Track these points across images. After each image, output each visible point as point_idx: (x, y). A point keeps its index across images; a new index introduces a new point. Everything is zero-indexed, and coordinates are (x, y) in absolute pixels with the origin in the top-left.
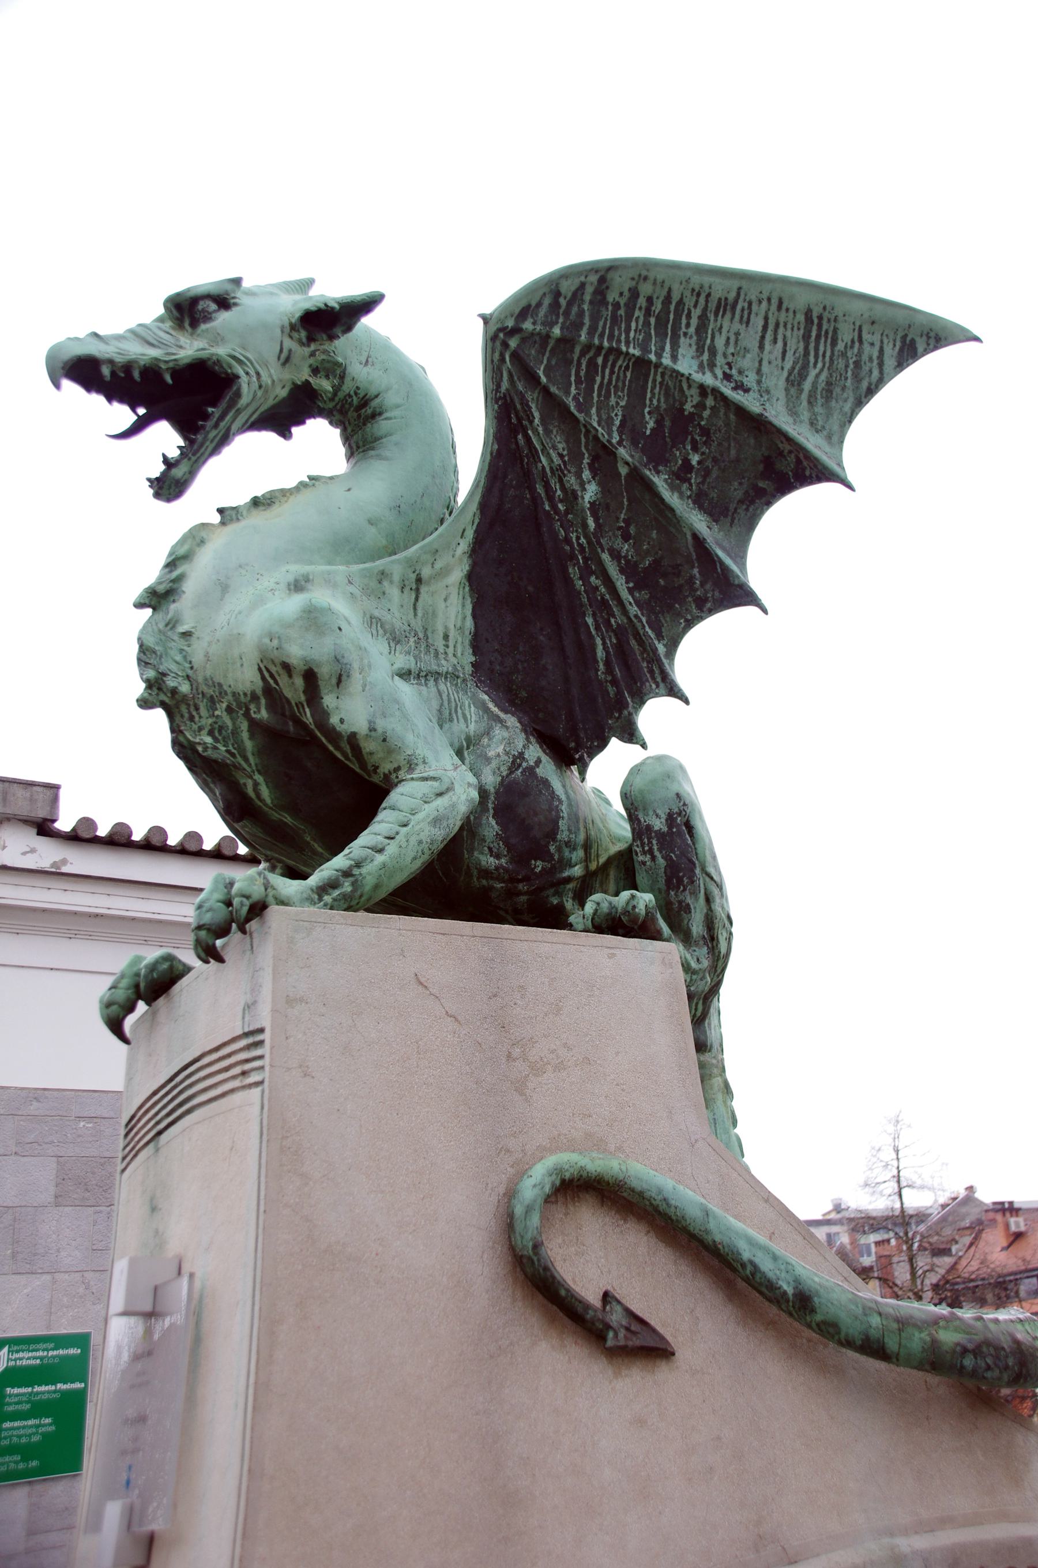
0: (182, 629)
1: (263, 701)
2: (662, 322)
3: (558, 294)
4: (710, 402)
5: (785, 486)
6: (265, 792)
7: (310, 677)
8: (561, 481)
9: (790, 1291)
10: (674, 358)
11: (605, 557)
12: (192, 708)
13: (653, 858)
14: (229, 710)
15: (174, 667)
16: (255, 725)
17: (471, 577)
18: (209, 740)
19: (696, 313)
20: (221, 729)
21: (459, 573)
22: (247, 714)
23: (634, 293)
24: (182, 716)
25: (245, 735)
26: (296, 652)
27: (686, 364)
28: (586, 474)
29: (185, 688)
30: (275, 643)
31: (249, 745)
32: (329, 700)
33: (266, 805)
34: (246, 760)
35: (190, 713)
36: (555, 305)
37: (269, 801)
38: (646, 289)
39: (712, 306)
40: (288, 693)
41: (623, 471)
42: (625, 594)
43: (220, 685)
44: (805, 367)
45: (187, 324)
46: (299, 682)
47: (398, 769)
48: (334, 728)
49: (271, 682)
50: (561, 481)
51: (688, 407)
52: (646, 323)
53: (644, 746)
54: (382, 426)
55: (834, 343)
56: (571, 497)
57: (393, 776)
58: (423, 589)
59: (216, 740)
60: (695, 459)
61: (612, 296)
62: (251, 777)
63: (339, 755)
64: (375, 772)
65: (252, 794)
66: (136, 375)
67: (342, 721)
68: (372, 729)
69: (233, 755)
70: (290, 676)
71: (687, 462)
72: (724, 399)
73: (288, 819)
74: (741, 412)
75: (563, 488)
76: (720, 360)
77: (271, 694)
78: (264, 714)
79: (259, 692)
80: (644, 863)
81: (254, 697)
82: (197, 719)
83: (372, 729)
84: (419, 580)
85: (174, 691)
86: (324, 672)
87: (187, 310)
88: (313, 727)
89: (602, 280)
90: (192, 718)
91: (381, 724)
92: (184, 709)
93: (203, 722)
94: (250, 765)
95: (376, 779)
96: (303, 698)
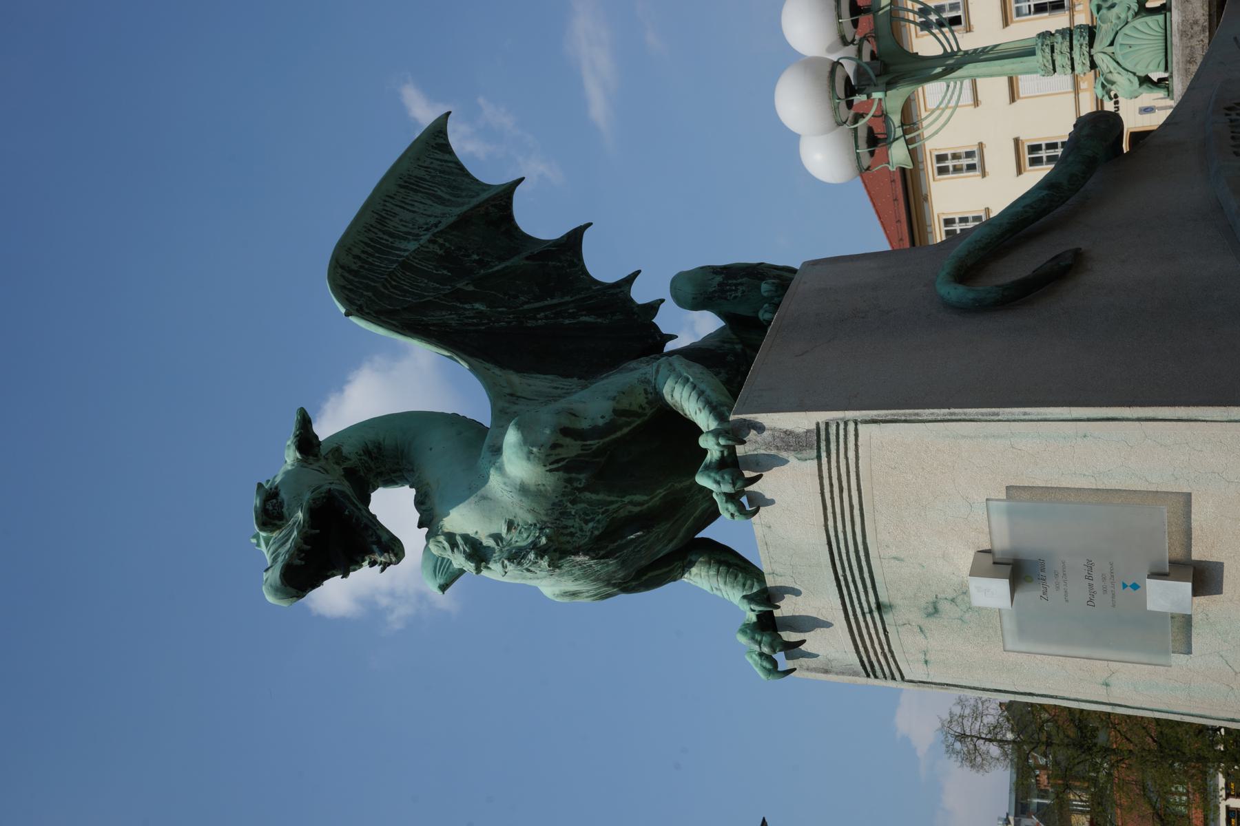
0: (504, 531)
1: (573, 475)
3: (344, 287)
4: (441, 241)
5: (510, 218)
6: (638, 498)
7: (566, 432)
9: (1045, 192)
10: (405, 251)
11: (526, 307)
12: (565, 532)
13: (741, 284)
14: (573, 502)
17: (519, 370)
18: (591, 525)
21: (515, 378)
22: (580, 490)
23: (356, 257)
25: (594, 497)
27: (412, 246)
31: (601, 497)
32: (585, 425)
33: (647, 502)
35: (567, 535)
36: (350, 290)
37: (646, 498)
38: (356, 251)
42: (555, 301)
43: (554, 504)
44: (433, 195)
52: (379, 258)
53: (662, 301)
55: (425, 180)
59: (592, 520)
60: (475, 257)
61: (354, 267)
63: (626, 430)
64: (644, 409)
67: (603, 417)
68: (614, 399)
71: (475, 261)
72: (441, 232)
73: (661, 492)
74: (453, 226)
76: (415, 231)
79: (566, 476)
81: (569, 481)
83: (614, 399)
84: (512, 395)
86: (566, 422)
88: (601, 442)
89: (342, 267)
90: (572, 534)
93: (577, 525)
95: (649, 412)
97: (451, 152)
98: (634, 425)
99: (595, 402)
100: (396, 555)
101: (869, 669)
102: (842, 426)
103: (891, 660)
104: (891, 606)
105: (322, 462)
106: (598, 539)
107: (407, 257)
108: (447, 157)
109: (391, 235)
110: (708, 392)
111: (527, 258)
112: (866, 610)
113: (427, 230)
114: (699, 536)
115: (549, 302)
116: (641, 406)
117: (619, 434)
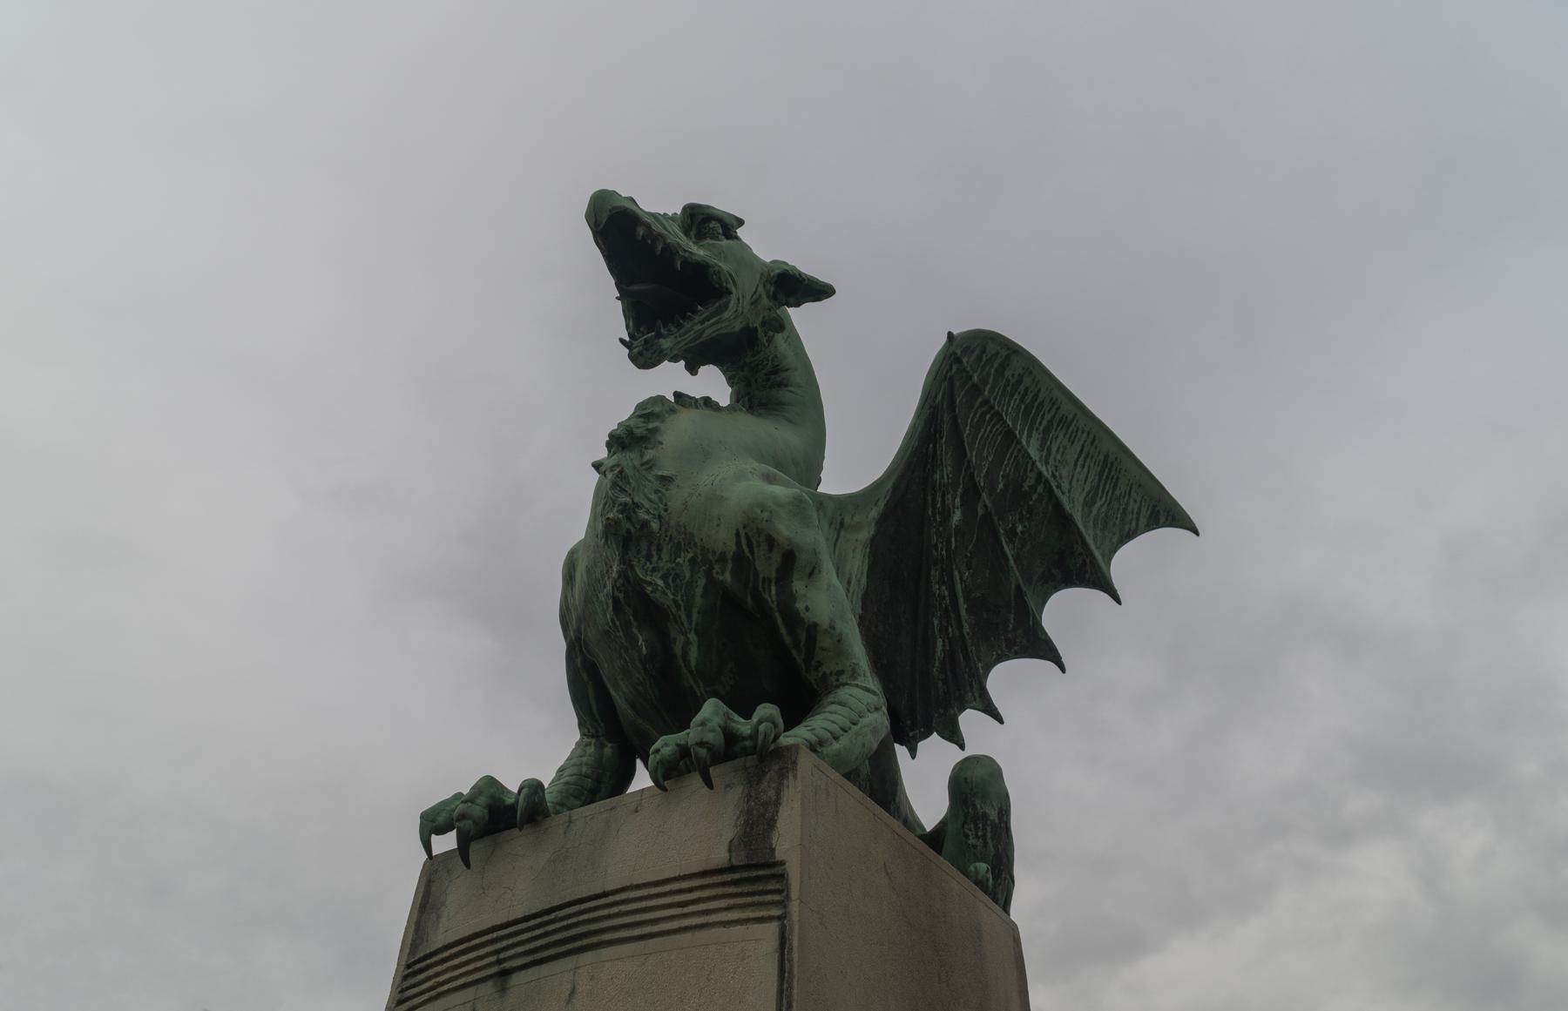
1: (730, 566)
2: (1027, 414)
4: (1040, 489)
5: (1069, 582)
6: (694, 653)
7: (789, 558)
8: (943, 496)
13: (985, 844)
14: (693, 561)
15: (646, 503)
16: (711, 581)
18: (660, 583)
19: (1048, 417)
20: (677, 576)
21: (866, 534)
22: (709, 573)
23: (1020, 381)
24: (639, 552)
25: (699, 591)
26: (785, 529)
27: (1033, 452)
28: (958, 500)
29: (655, 525)
30: (766, 515)
31: (698, 601)
32: (798, 586)
33: (687, 666)
34: (689, 616)
35: (649, 550)
37: (693, 664)
38: (1027, 381)
39: (1058, 417)
40: (760, 565)
41: (980, 512)
42: (963, 613)
43: (692, 535)
44: (1096, 495)
45: (692, 233)
46: (776, 558)
47: (841, 673)
48: (797, 613)
49: (746, 549)
50: (943, 496)
51: (1026, 485)
53: (962, 747)
54: (784, 395)
56: (947, 514)
57: (833, 678)
58: (843, 533)
59: (667, 585)
60: (1020, 528)
61: (1008, 374)
62: (684, 634)
63: (788, 640)
64: (816, 669)
65: (678, 649)
66: (659, 247)
67: (807, 609)
69: (678, 607)
70: (771, 549)
71: (1014, 527)
72: (1051, 491)
74: (1058, 505)
75: (943, 501)
76: (1051, 461)
77: (742, 562)
78: (727, 577)
79: (730, 556)
80: (974, 847)
81: (722, 558)
82: (655, 559)
83: (832, 627)
85: (645, 524)
87: (701, 221)
88: (774, 606)
89: (1007, 358)
90: (649, 557)
91: (839, 625)
92: (644, 545)
94: (690, 622)
96: (773, 575)
97: (1149, 528)
98: (794, 652)
99: (832, 599)
100: (640, 354)
101: (418, 966)
102: (777, 897)
103: (426, 996)
104: (503, 990)
105: (765, 301)
106: (643, 596)
107: (1019, 442)
108: (1143, 522)
109: (1047, 431)
110: (836, 746)
111: (1018, 587)
112: (502, 956)
113: (1054, 476)
114: (639, 763)
115: (963, 607)
116: (820, 664)
117: (783, 631)
